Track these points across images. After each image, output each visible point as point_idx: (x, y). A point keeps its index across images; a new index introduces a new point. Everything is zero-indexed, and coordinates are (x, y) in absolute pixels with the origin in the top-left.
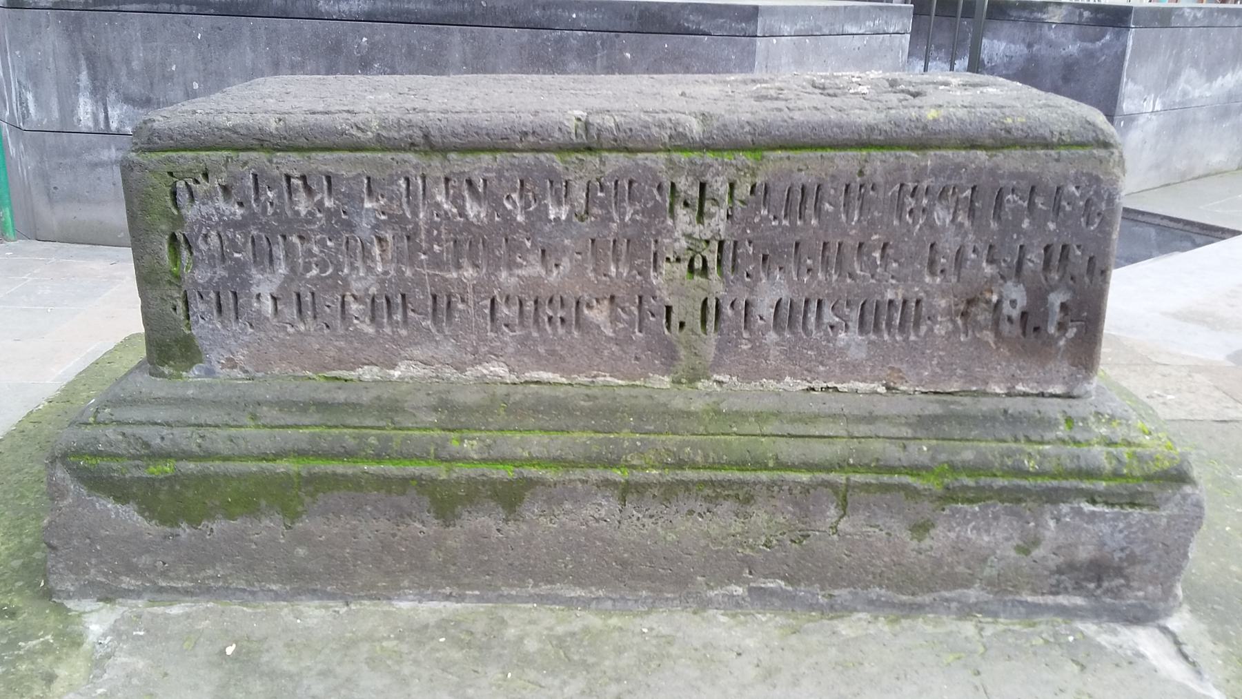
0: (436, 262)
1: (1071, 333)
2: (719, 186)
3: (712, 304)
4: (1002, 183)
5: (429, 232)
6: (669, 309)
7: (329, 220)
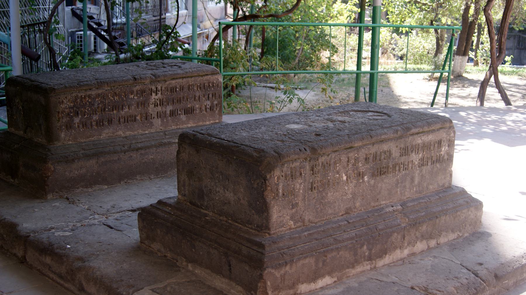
0: (109, 110)
1: (218, 109)
2: (159, 88)
3: (159, 112)
4: (204, 82)
5: (108, 104)
6: (151, 114)
7: (89, 104)
